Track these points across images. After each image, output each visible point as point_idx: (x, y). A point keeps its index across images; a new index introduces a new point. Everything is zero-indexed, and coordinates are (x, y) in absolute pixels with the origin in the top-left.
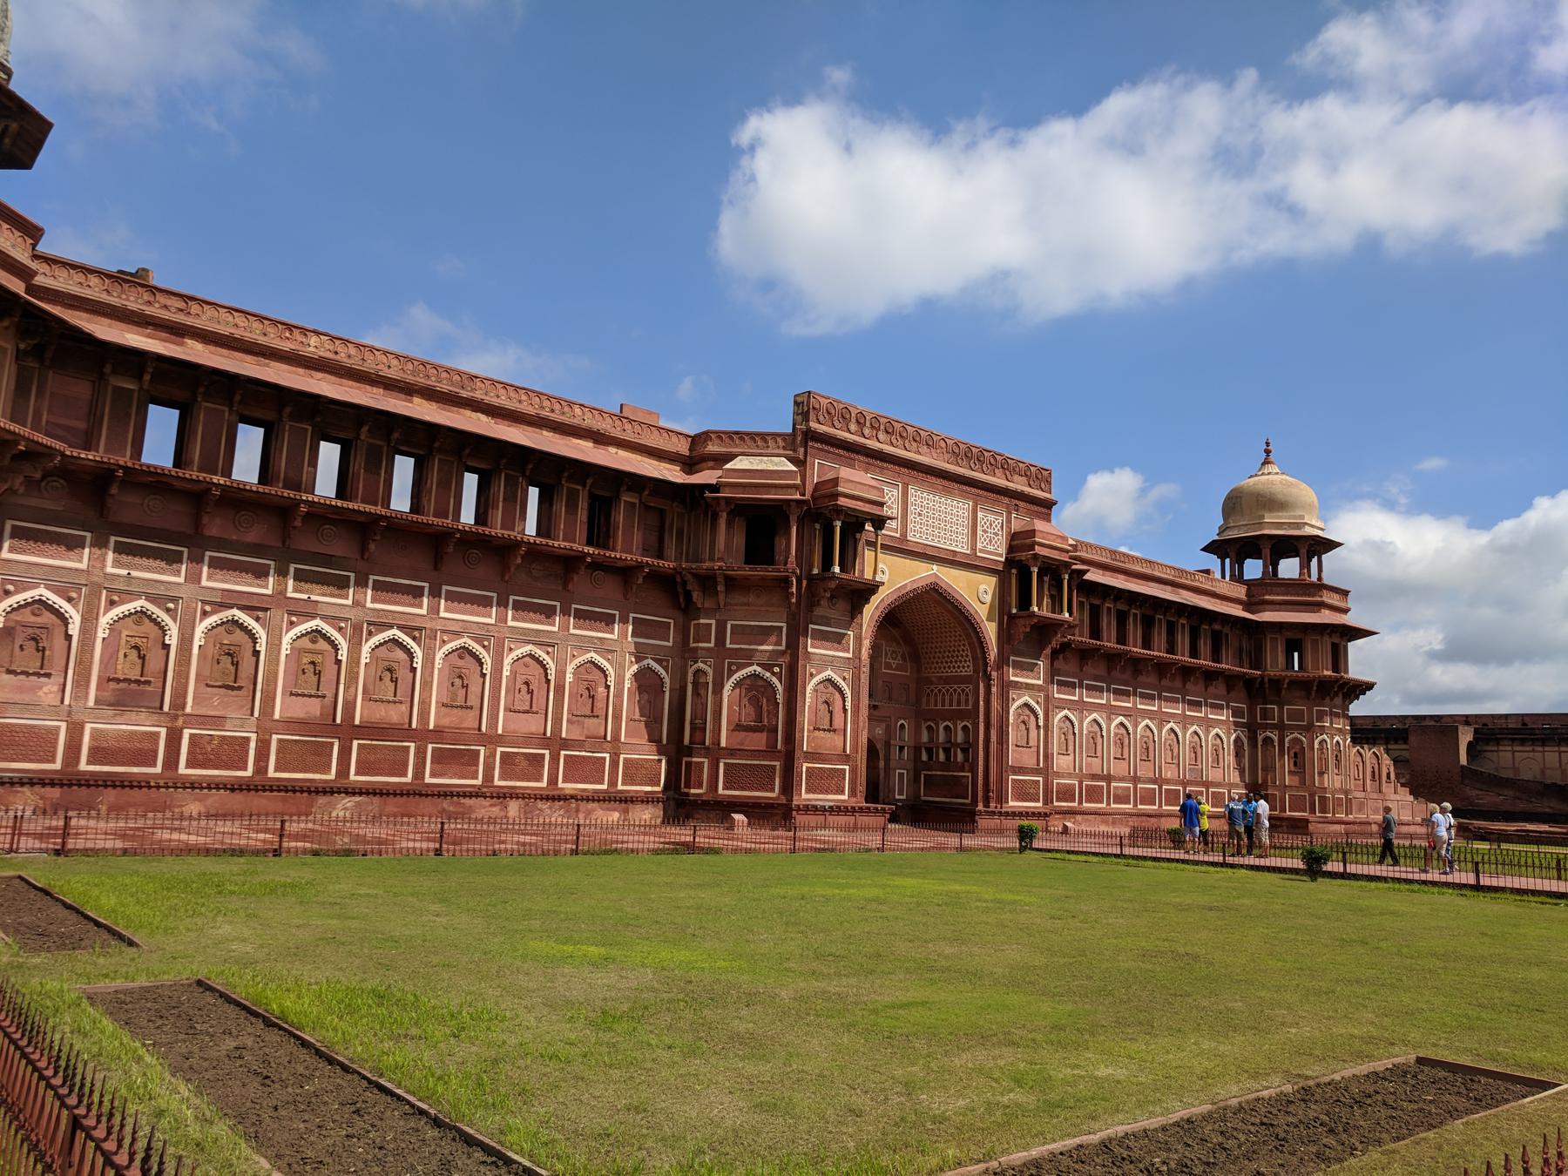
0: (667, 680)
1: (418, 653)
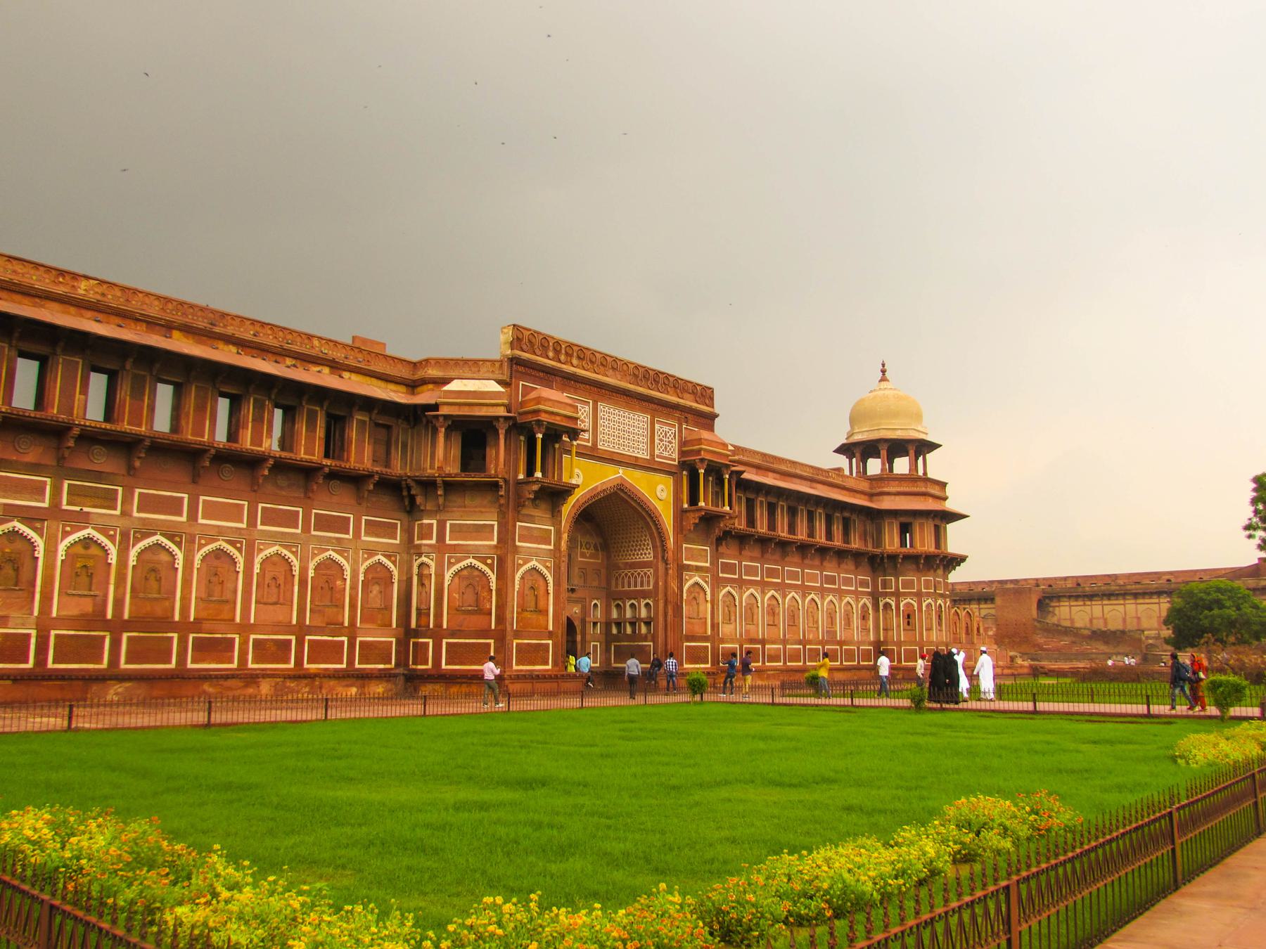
0: (396, 573)
1: (180, 556)
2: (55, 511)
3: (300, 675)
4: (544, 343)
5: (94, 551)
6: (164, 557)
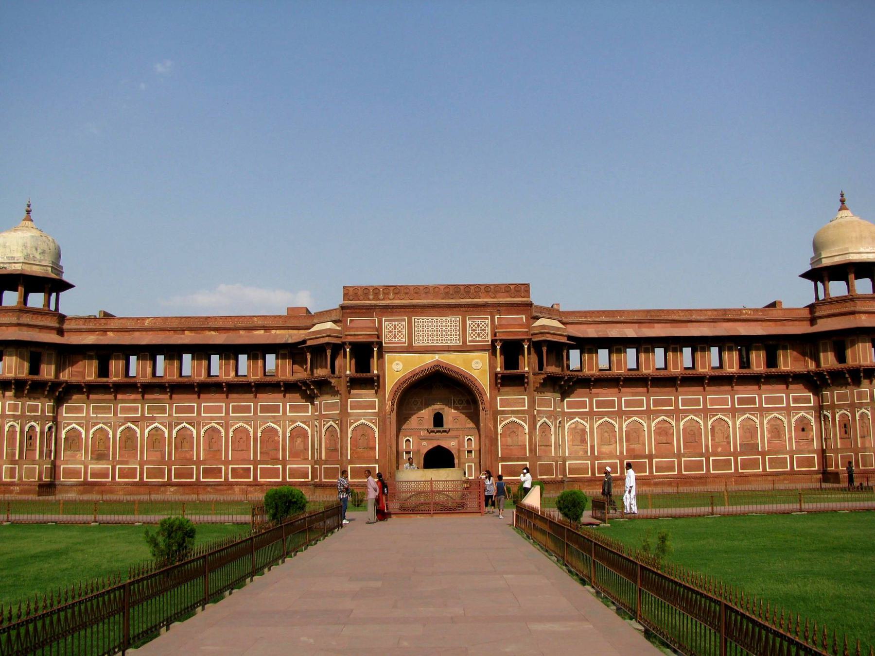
0: (309, 431)
3: (256, 484)
5: (159, 432)
6: (189, 432)
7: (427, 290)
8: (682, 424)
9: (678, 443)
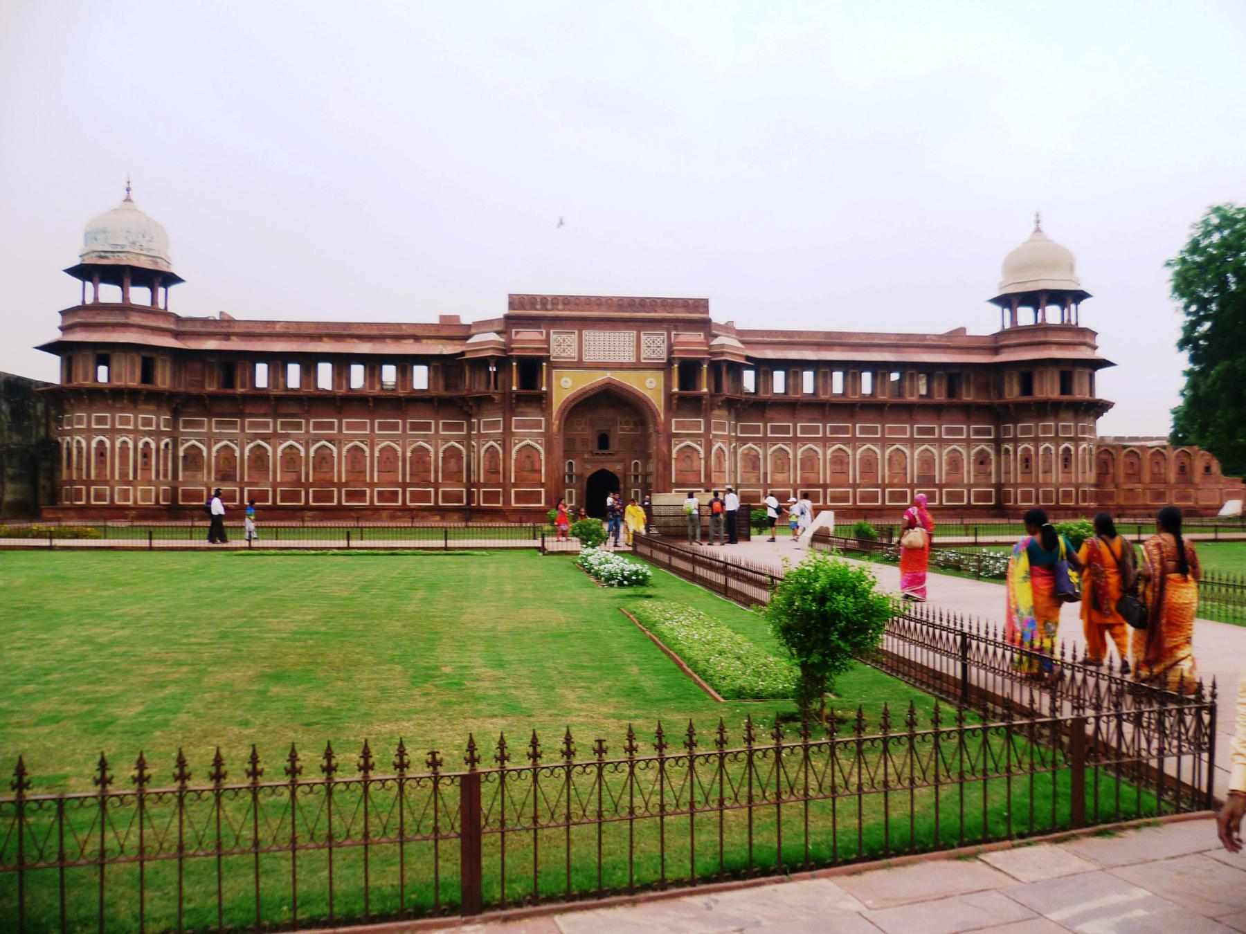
0: (464, 451)
1: (335, 450)
2: (275, 434)
3: (404, 509)
4: (531, 301)
7: (600, 302)
8: (859, 452)
9: (854, 472)
